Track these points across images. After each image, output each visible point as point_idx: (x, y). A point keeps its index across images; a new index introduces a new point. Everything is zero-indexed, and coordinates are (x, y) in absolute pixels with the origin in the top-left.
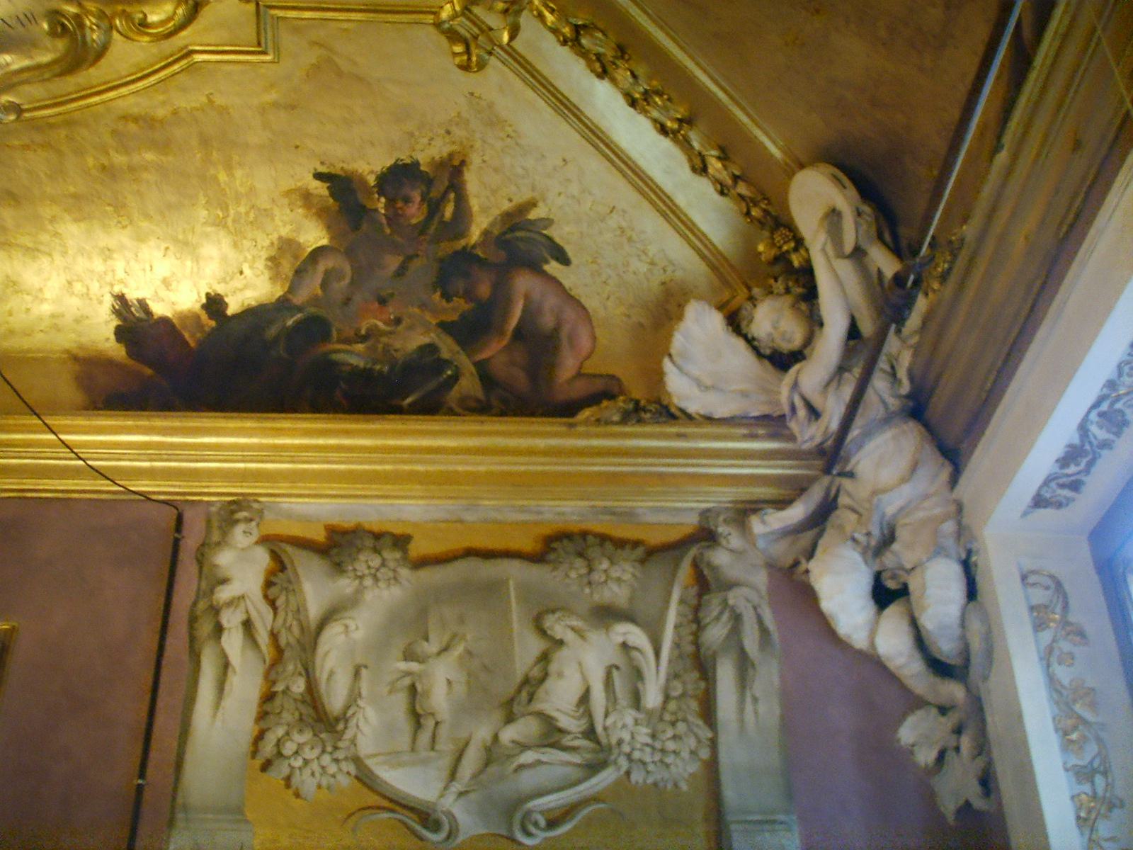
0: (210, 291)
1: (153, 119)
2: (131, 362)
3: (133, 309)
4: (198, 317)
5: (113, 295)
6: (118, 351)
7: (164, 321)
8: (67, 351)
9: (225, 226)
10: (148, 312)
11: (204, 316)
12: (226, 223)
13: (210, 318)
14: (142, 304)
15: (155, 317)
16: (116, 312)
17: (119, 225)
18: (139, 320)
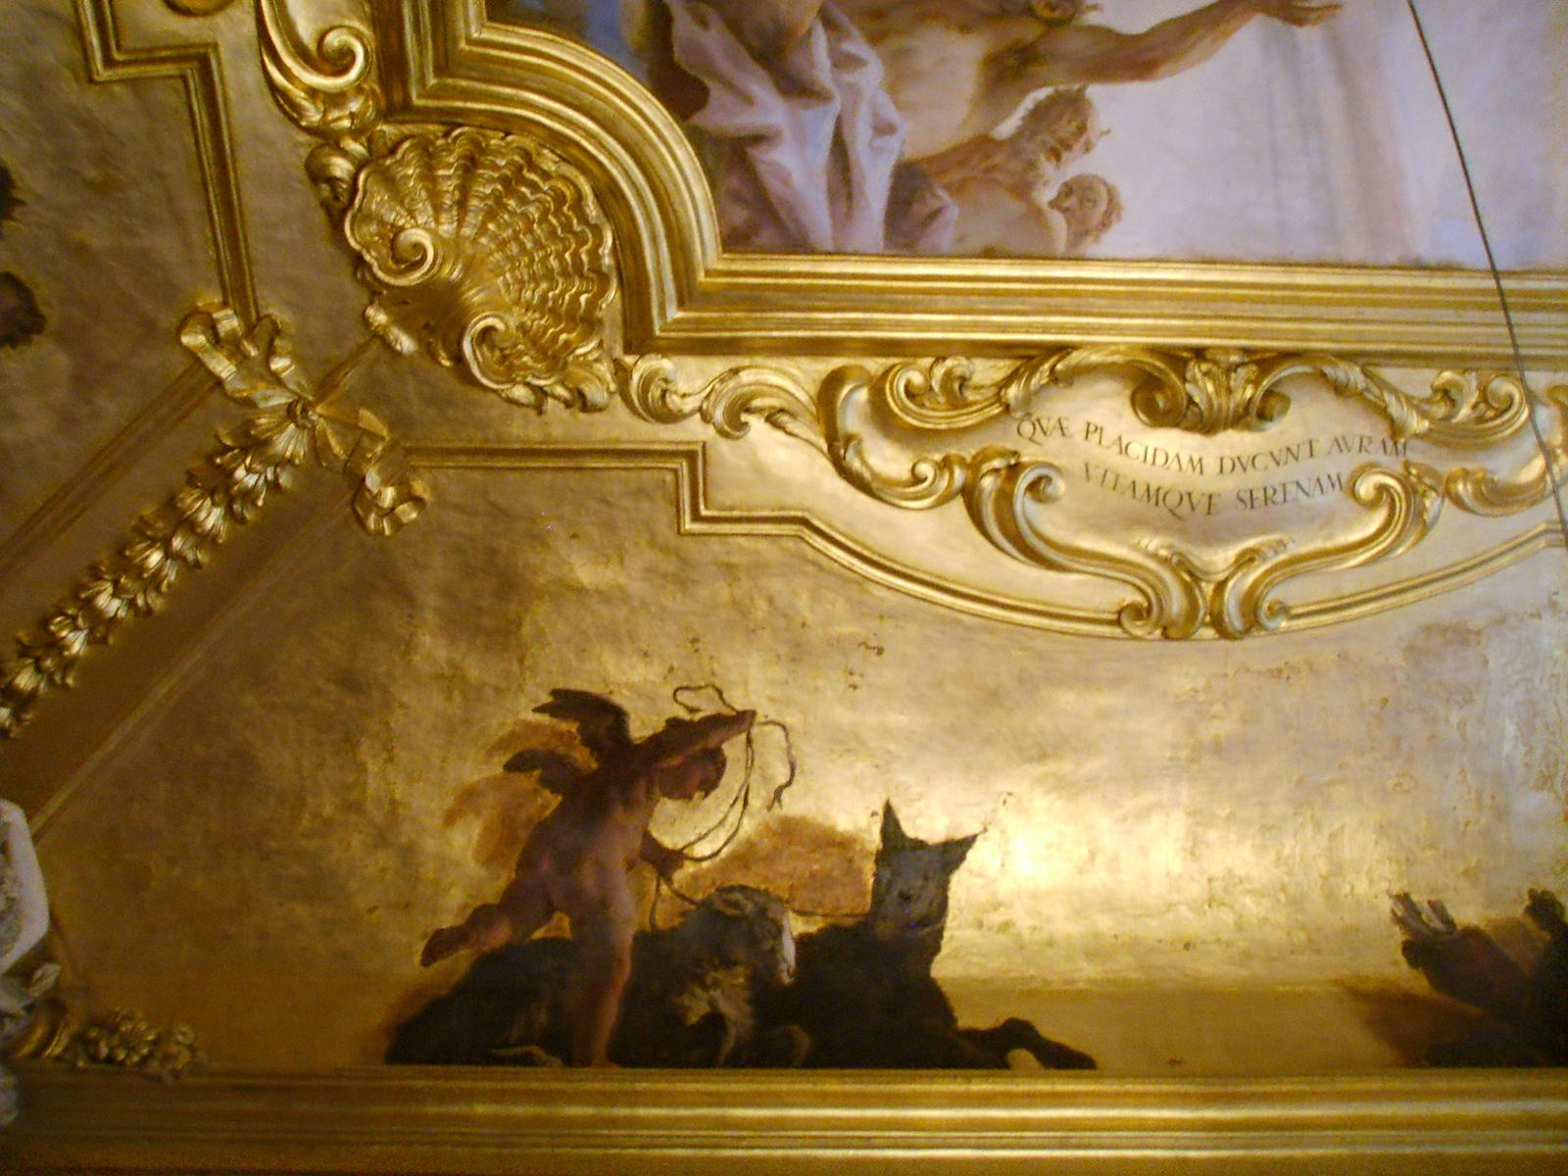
0: (1534, 887)
1: (1469, 631)
2: (1436, 996)
3: (1424, 916)
4: (1518, 926)
5: (1391, 896)
6: (1414, 981)
7: (1471, 933)
8: (1336, 982)
9: (1552, 789)
10: (1449, 922)
11: (1530, 923)
12: (1552, 785)
13: (1543, 928)
14: (1437, 908)
15: (1459, 928)
16: (1398, 920)
17: (1399, 789)
18: (1436, 932)
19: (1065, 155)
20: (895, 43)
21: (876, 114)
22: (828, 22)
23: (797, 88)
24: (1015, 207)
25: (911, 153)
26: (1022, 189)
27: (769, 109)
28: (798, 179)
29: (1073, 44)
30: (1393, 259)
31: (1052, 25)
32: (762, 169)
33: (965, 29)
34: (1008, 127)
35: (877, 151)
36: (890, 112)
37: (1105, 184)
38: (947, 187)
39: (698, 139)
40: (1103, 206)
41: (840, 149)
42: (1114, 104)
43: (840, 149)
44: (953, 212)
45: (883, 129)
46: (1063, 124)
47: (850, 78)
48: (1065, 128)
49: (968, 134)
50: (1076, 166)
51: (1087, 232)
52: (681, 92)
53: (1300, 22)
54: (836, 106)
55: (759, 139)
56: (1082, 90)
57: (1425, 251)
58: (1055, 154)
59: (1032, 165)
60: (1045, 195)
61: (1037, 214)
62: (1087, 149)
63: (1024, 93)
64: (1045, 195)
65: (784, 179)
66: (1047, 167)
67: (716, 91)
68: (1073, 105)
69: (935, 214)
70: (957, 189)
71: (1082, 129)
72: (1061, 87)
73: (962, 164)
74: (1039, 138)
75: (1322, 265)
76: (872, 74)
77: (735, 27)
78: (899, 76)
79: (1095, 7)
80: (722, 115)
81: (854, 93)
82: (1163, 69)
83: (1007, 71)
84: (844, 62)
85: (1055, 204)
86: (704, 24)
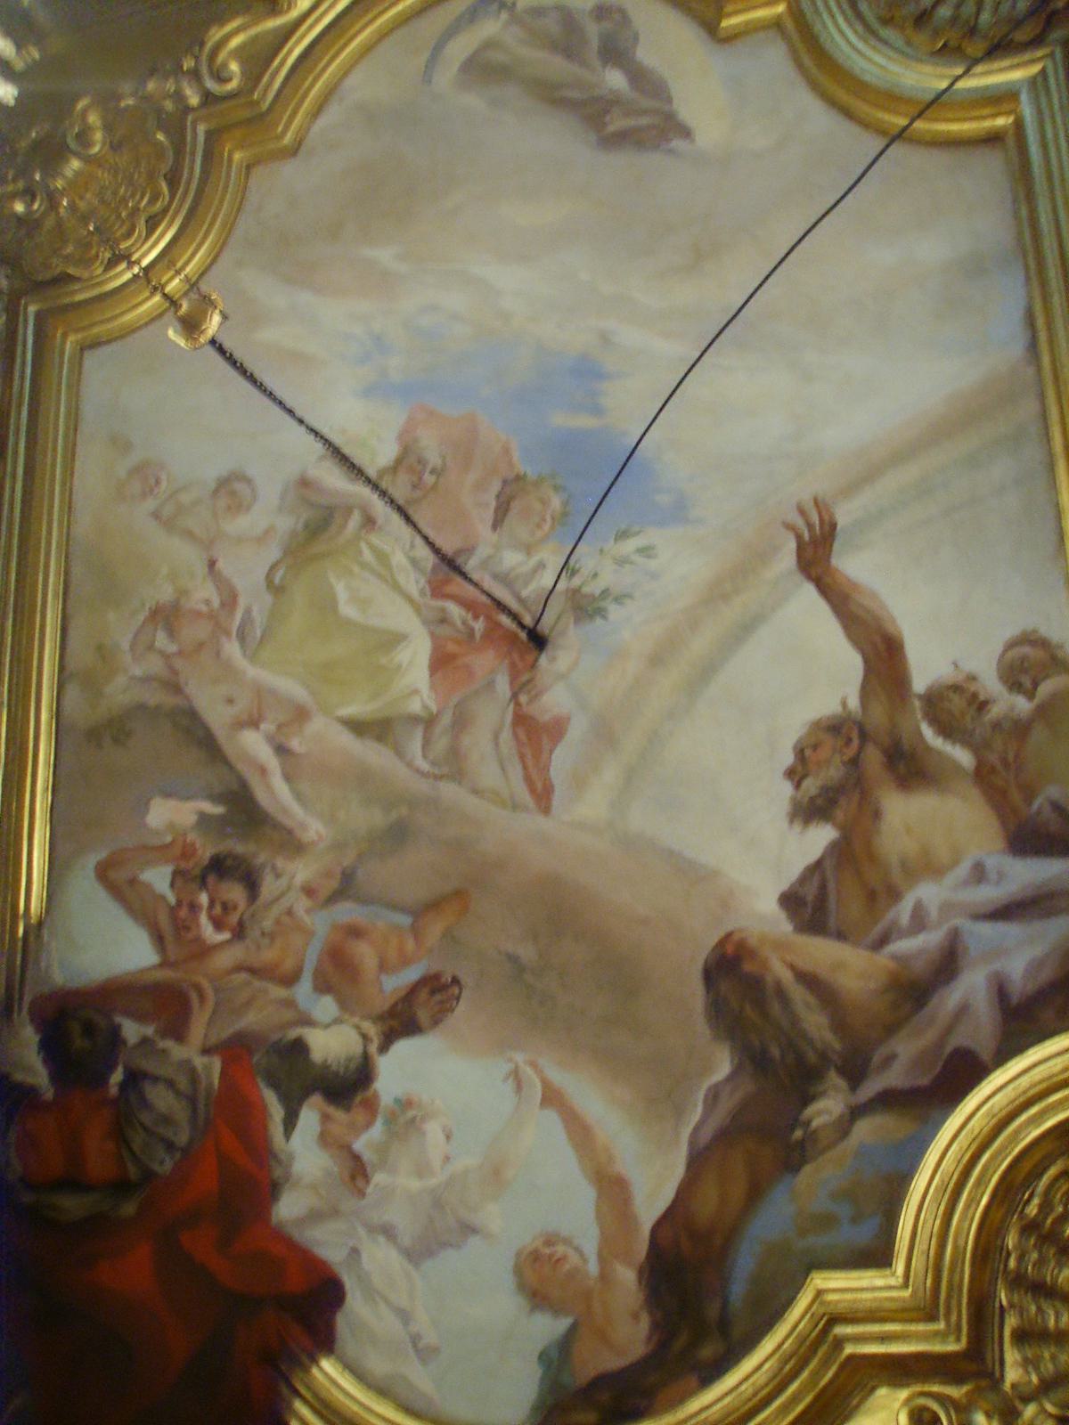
19: (982, 698)
20: (896, 876)
21: (966, 883)
22: (882, 941)
23: (948, 963)
24: (1039, 734)
25: (1000, 843)
26: (1020, 729)
27: (971, 987)
28: (1037, 951)
29: (878, 716)
30: (1031, 371)
31: (864, 736)
32: (1031, 987)
33: (877, 815)
34: (963, 756)
35: (1001, 876)
36: (963, 869)
37: (1005, 651)
38: (1029, 799)
39: (1002, 1057)
40: (1026, 650)
41: (1005, 912)
42: (927, 667)
43: (1005, 912)
44: (1053, 791)
45: (979, 874)
46: (954, 707)
47: (934, 913)
48: (957, 703)
49: (975, 794)
50: (991, 684)
51: (1054, 658)
52: (958, 1074)
53: (833, 526)
54: (958, 921)
55: (1001, 991)
56: (920, 697)
57: (1017, 349)
58: (983, 706)
59: (996, 726)
60: (1023, 705)
61: (1042, 711)
62: (972, 678)
63: (929, 749)
64: (1023, 705)
65: (1035, 966)
66: (995, 711)
67: (956, 1041)
68: (935, 702)
69: (1057, 807)
70: (1029, 793)
71: (956, 688)
72: (919, 716)
73: (1004, 793)
74: (970, 727)
75: (1047, 434)
76: (928, 893)
77: (891, 1029)
78: (927, 867)
79: (844, 704)
80: (981, 1031)
81: (947, 908)
82: (891, 630)
83: (910, 768)
84: (919, 922)
85: (1030, 695)
86: (890, 1059)
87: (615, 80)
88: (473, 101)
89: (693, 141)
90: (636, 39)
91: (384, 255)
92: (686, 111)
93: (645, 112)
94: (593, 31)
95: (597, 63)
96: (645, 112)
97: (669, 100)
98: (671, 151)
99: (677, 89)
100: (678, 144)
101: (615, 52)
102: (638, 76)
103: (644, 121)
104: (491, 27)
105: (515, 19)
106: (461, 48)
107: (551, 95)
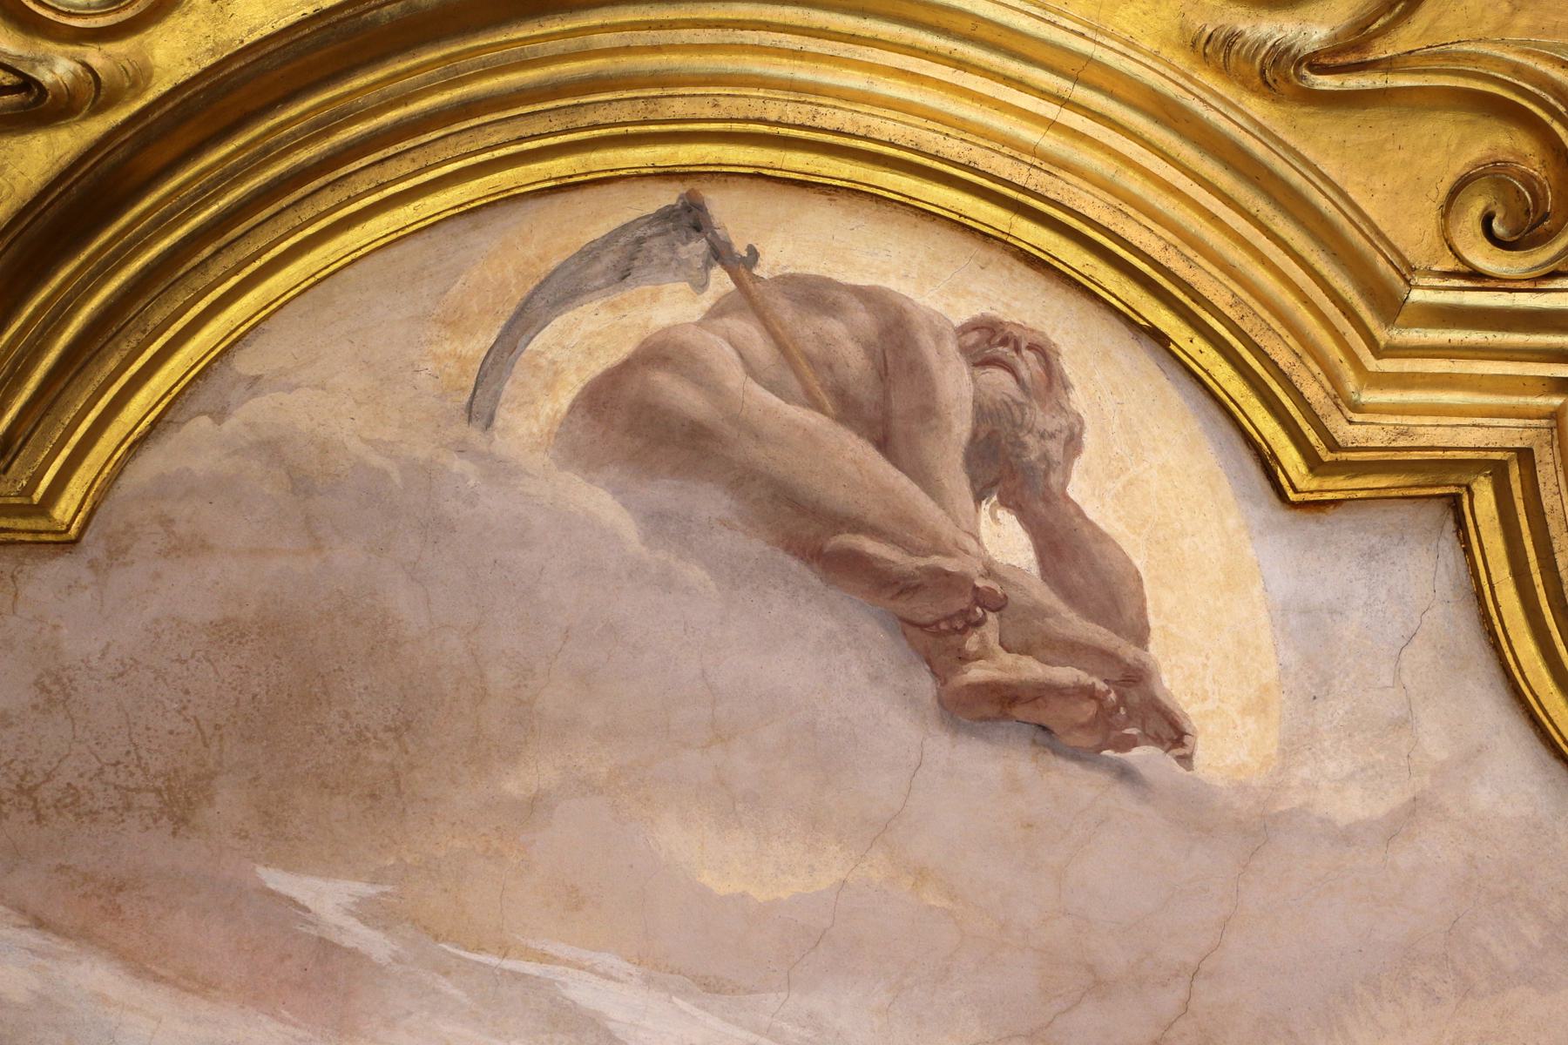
87: (1004, 541)
88: (600, 504)
89: (1186, 760)
90: (1073, 443)
91: (327, 898)
92: (1180, 673)
93: (1073, 650)
94: (956, 385)
95: (957, 483)
96: (1073, 650)
97: (1140, 635)
98: (1125, 774)
99: (1165, 607)
100: (1144, 756)
101: (1010, 464)
102: (1062, 542)
103: (1065, 674)
104: (672, 305)
105: (749, 298)
106: (587, 340)
107: (821, 543)
